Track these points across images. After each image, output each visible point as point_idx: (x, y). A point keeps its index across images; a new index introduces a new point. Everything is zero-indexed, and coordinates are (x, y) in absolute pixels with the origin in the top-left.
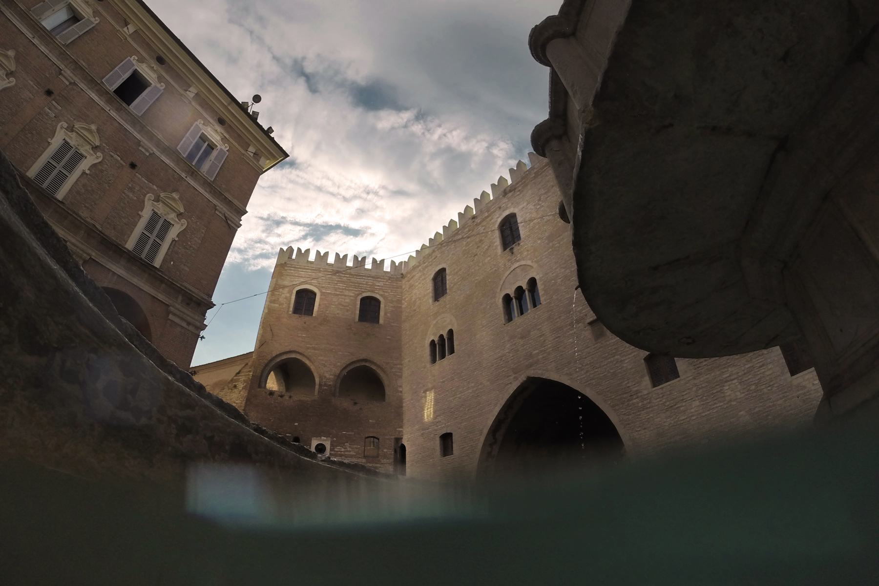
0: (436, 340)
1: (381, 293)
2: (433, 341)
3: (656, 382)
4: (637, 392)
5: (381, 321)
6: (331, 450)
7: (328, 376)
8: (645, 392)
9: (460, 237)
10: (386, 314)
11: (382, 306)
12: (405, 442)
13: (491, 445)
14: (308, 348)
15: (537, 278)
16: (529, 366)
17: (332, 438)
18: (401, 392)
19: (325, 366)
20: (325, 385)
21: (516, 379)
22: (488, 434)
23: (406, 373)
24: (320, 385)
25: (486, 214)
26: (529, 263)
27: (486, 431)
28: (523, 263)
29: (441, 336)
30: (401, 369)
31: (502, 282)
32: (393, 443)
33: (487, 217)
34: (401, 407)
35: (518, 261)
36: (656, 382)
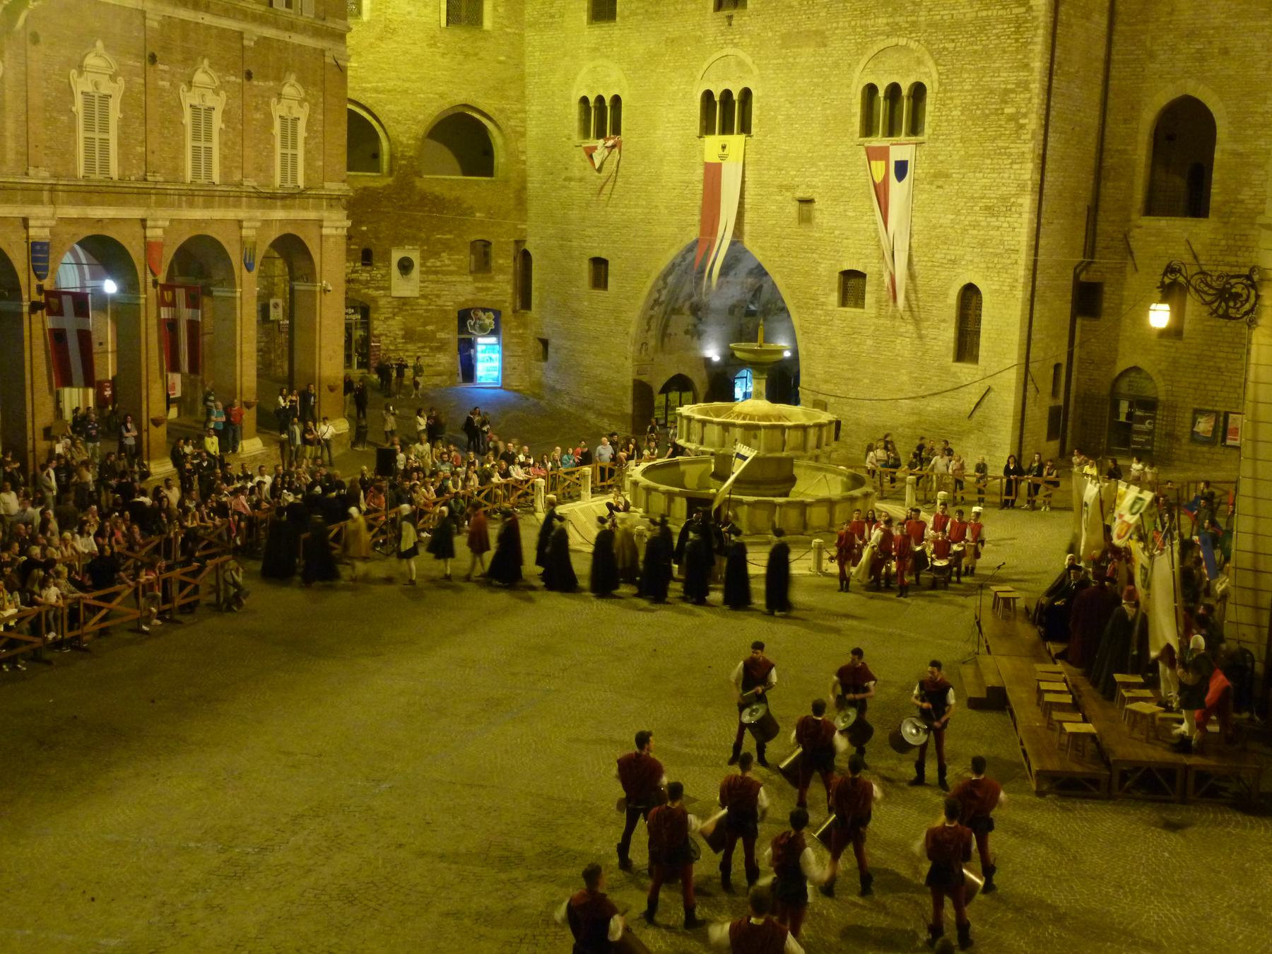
0: (592, 100)
2: (584, 100)
3: (844, 302)
4: (823, 304)
5: (488, 23)
6: (422, 265)
7: (404, 139)
8: (830, 308)
10: (495, 8)
12: (529, 246)
13: (659, 291)
14: (365, 90)
15: (754, 93)
17: (421, 246)
18: (524, 162)
19: (399, 122)
20: (403, 157)
22: (658, 279)
23: (533, 131)
24: (392, 157)
26: (749, 60)
27: (655, 275)
28: (742, 54)
29: (600, 99)
30: (523, 121)
31: (705, 67)
32: (512, 247)
34: (524, 188)
35: (736, 45)
36: (844, 302)
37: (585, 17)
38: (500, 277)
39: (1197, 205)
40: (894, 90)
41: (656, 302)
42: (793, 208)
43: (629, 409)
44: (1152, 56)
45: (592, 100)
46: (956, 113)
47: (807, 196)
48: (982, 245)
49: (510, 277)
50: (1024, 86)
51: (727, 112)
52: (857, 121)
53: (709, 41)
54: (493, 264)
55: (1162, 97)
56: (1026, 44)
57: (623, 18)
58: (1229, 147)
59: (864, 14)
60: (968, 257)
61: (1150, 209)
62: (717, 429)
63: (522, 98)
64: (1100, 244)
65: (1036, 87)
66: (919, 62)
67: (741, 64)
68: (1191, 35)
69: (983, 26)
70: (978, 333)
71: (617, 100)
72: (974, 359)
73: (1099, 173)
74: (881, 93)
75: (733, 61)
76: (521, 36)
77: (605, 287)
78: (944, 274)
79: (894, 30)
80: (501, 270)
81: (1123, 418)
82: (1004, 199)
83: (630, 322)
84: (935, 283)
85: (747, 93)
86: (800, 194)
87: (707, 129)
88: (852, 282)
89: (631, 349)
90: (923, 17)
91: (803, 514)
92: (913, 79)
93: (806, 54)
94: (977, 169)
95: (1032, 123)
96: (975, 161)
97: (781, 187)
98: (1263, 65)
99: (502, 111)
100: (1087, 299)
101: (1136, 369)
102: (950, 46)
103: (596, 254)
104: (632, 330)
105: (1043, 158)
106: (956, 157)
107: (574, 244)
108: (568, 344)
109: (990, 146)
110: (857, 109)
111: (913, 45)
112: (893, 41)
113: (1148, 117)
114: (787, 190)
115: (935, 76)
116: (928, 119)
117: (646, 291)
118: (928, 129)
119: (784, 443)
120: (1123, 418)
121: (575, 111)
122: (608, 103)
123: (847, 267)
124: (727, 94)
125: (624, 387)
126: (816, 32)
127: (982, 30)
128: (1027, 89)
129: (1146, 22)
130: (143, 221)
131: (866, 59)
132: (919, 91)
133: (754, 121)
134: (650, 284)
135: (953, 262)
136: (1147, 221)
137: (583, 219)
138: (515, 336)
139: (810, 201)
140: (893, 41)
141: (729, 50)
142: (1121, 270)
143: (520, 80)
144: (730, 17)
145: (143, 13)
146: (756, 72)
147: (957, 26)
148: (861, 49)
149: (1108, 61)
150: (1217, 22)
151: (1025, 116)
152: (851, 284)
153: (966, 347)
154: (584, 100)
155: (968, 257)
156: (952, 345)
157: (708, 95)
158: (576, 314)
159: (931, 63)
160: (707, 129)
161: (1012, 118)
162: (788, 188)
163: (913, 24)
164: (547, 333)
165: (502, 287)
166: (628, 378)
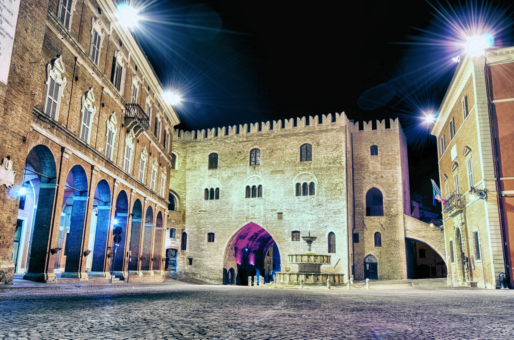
0: (209, 189)
1: (177, 151)
2: (206, 190)
9: (228, 142)
11: (177, 159)
15: (263, 186)
16: (253, 218)
21: (247, 221)
23: (188, 198)
25: (245, 139)
26: (261, 178)
27: (231, 237)
29: (212, 189)
30: (185, 195)
33: (246, 141)
34: (184, 214)
37: (207, 167)
38: (178, 240)
39: (380, 213)
40: (305, 184)
41: (230, 245)
42: (276, 216)
43: (222, 277)
44: (364, 178)
45: (209, 189)
46: (323, 189)
47: (281, 211)
48: (334, 222)
49: (180, 240)
50: (342, 182)
51: (253, 192)
52: (295, 192)
53: (248, 173)
54: (176, 236)
55: (368, 188)
56: (341, 173)
57: (220, 168)
58: (386, 199)
59: (295, 166)
60: (330, 225)
61: (369, 214)
62: (306, 257)
63: (185, 189)
64: (357, 223)
65: (345, 183)
66: (312, 177)
67: (258, 179)
68: (373, 173)
69: (329, 169)
70: (335, 245)
71: (218, 189)
72: (335, 252)
73: (354, 206)
74: (302, 185)
75: (256, 178)
76: (185, 172)
77: (213, 241)
78: (323, 230)
79: (304, 170)
80: (178, 238)
81: (368, 269)
82: (339, 210)
83: (222, 251)
84: (321, 232)
85: (260, 186)
86: (278, 211)
87: (248, 196)
88: (294, 234)
89: (222, 259)
90: (312, 166)
91: (334, 278)
92: (310, 181)
93: (279, 176)
94: (330, 202)
95: (344, 191)
96: (330, 201)
97: (272, 210)
98: (392, 180)
99: (180, 192)
100: (356, 238)
101: (370, 255)
102: (320, 173)
103: (210, 232)
104: (223, 253)
105: (347, 199)
106: (324, 200)
107: (203, 229)
108: (199, 259)
109: (333, 197)
110: (294, 189)
111: (310, 173)
112: (304, 172)
113: (365, 192)
114: (274, 210)
115: (317, 181)
116: (315, 191)
117: (228, 241)
118: (316, 194)
119: (324, 260)
120: (368, 269)
121: (203, 193)
122: (215, 190)
123: (294, 230)
124: (254, 187)
125: (220, 270)
126: (281, 171)
127: (329, 169)
128: (342, 183)
129: (362, 170)
130: (145, 198)
131: (296, 177)
132: (312, 184)
133: (263, 193)
134: (229, 239)
135: (326, 226)
136: (367, 217)
137: (206, 222)
138: (181, 258)
139: (282, 213)
140: (304, 172)
141: (255, 175)
142: (363, 230)
143: (184, 184)
144: (255, 167)
145: (150, 142)
146: (263, 180)
147: (322, 168)
148: (295, 175)
149: (353, 180)
150: (379, 171)
151: (342, 189)
152: (295, 235)
153: (331, 248)
154: (206, 190)
155: (330, 225)
156: (328, 248)
157: (248, 187)
158: (202, 250)
159: (315, 178)
160: (248, 196)
161: (340, 190)
162: (274, 210)
163: (310, 168)
164: (192, 256)
165: (177, 244)
166: (221, 268)
